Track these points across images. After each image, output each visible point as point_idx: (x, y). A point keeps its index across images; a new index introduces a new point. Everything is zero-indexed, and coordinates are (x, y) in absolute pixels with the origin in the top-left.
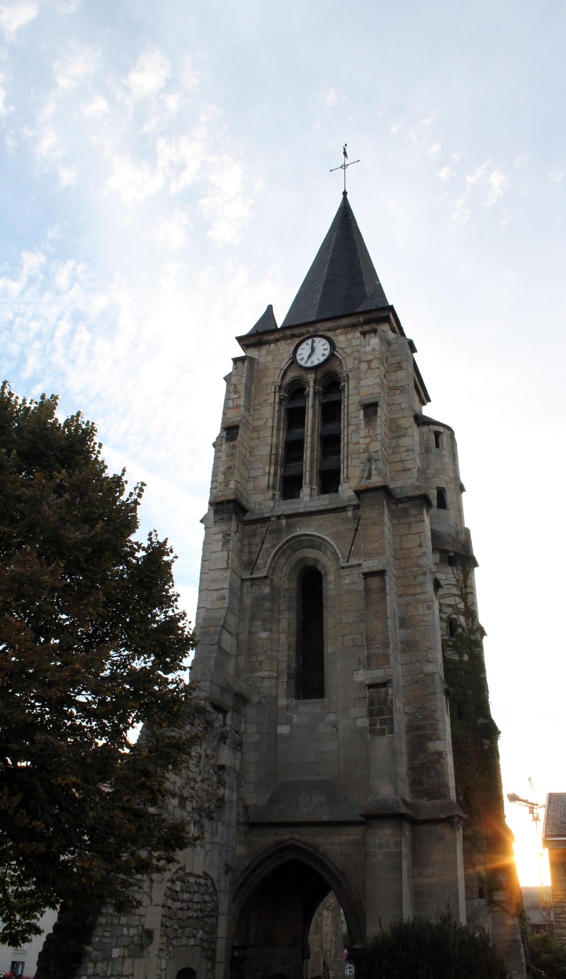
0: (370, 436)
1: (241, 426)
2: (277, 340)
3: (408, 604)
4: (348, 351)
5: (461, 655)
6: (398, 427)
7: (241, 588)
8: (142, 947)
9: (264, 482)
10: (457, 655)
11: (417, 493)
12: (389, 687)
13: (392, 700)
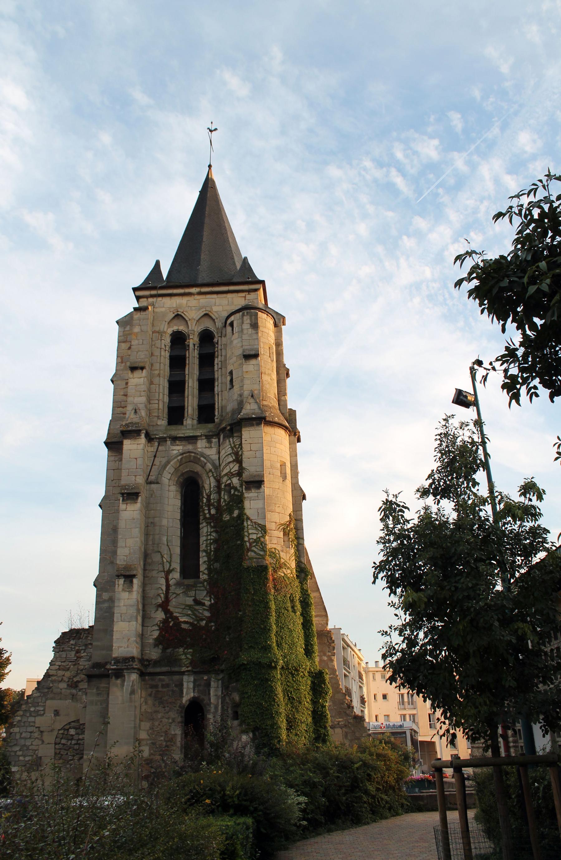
5: (231, 512)
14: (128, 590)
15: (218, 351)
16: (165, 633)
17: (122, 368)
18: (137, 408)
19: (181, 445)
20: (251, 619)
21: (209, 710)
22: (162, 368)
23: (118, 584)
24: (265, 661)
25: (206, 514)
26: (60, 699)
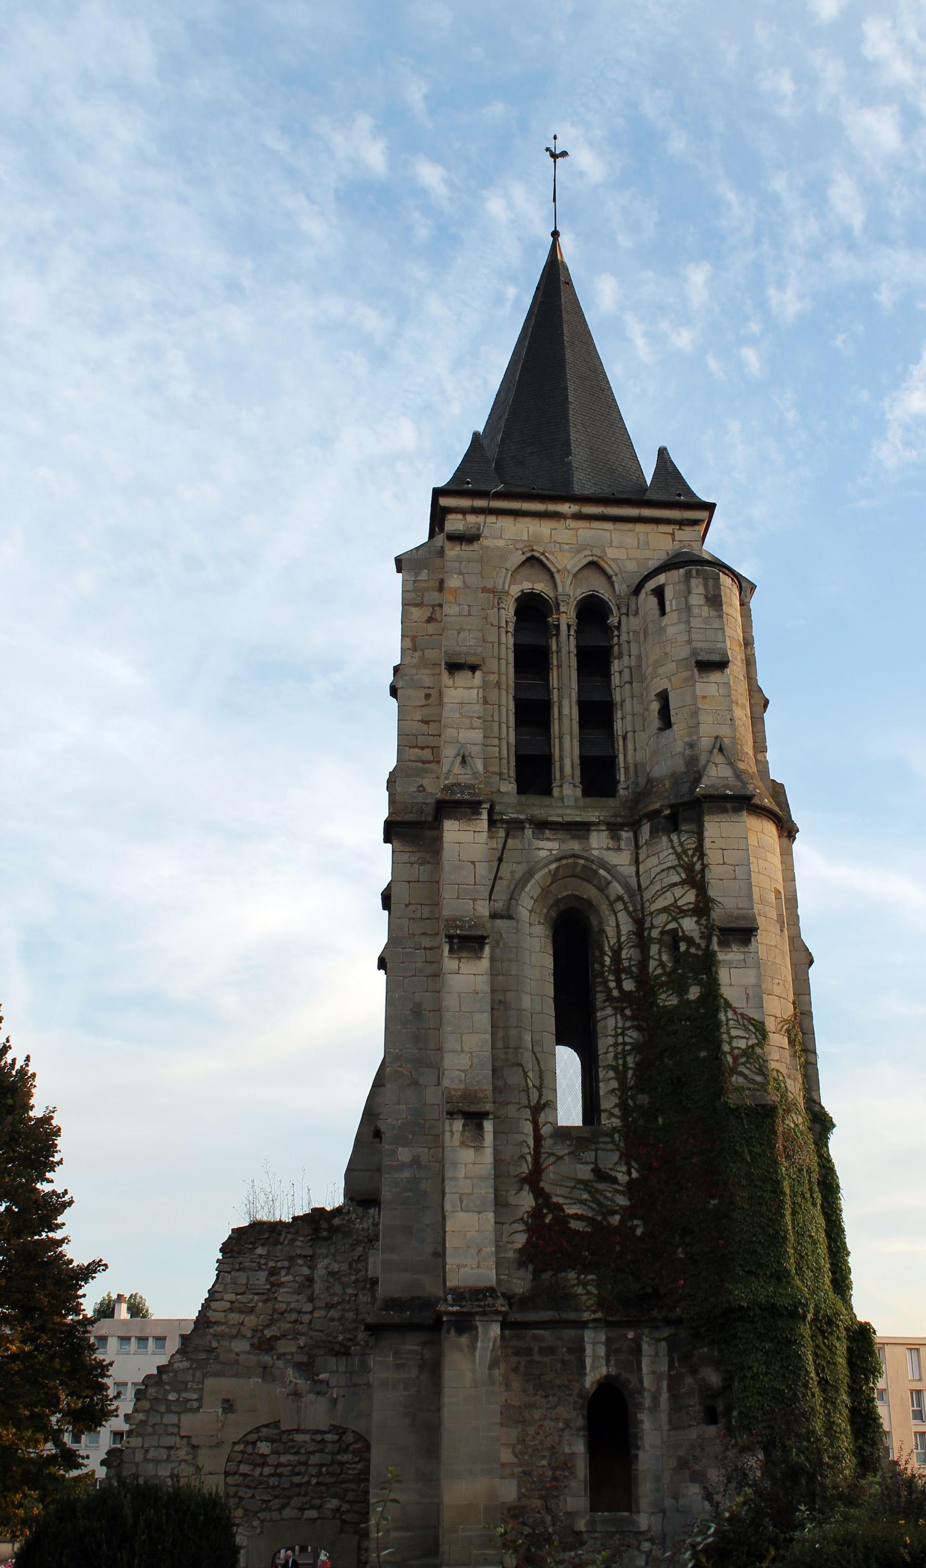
5: (682, 990)
14: (472, 1144)
15: (619, 644)
16: (537, 1239)
17: (415, 661)
18: (466, 754)
19: (555, 839)
20: (748, 1215)
21: (641, 1404)
22: (503, 670)
23: (451, 1131)
24: (782, 1302)
25: (612, 989)
26: (236, 1375)
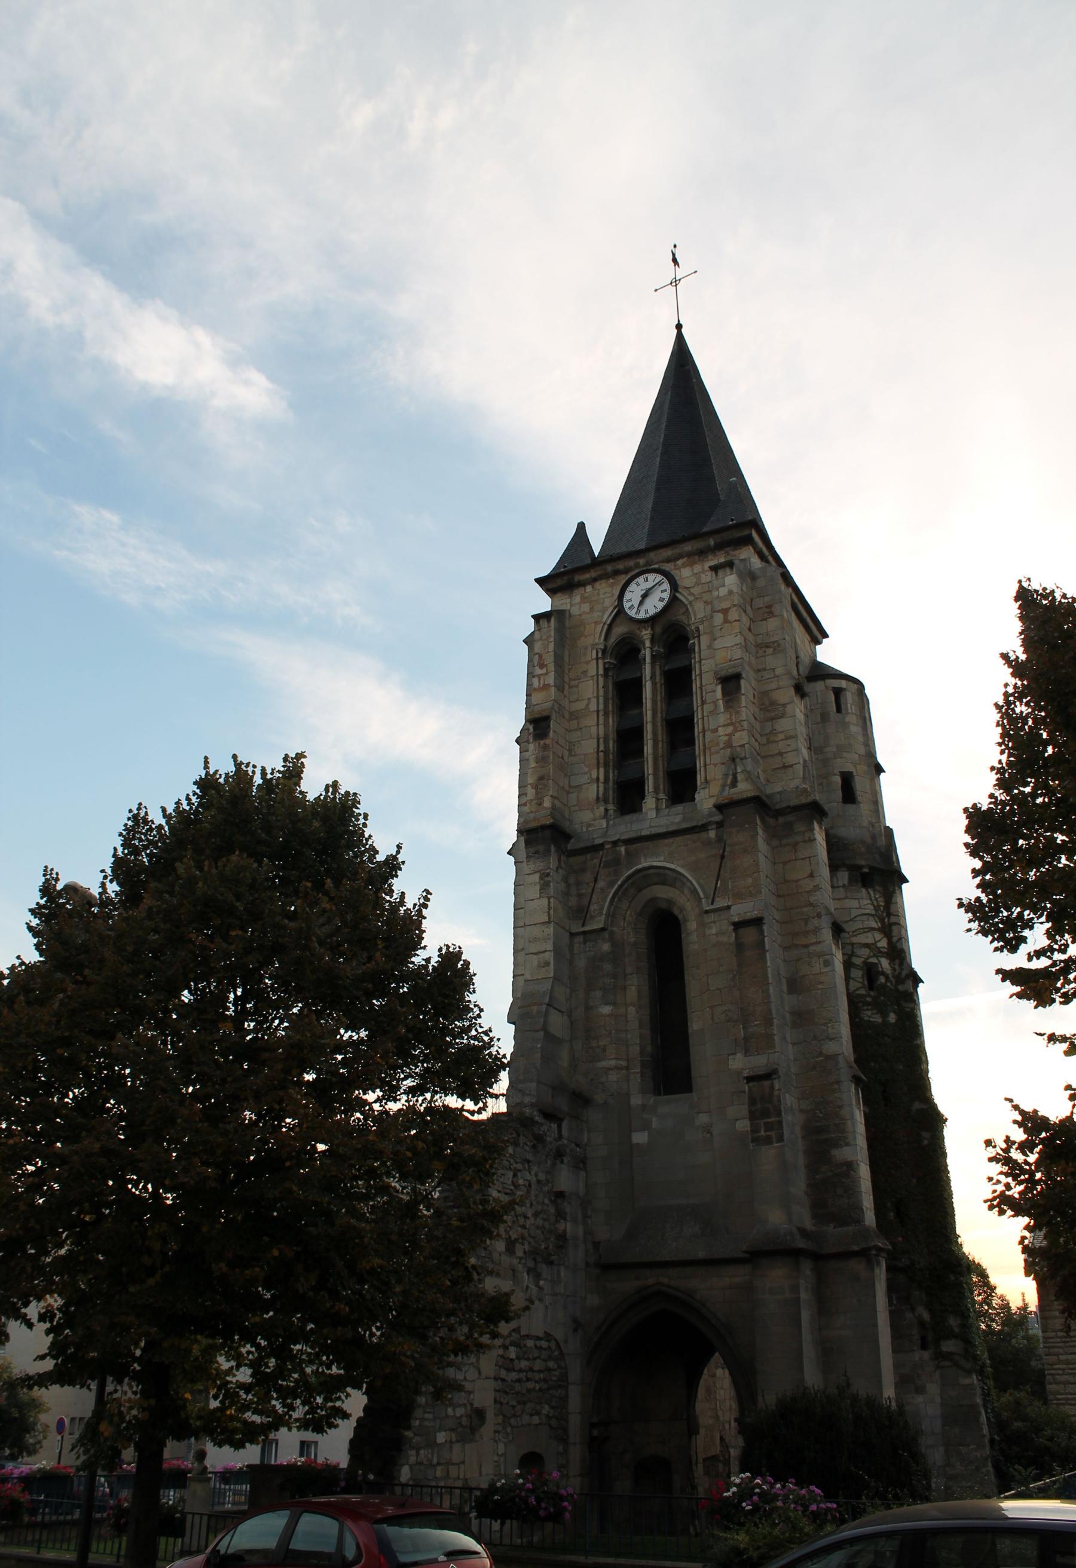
0: (731, 724)
1: (554, 716)
2: (595, 580)
3: (799, 960)
4: (696, 591)
5: (884, 1015)
6: (773, 703)
7: (571, 946)
8: (473, 1430)
9: (592, 792)
10: (879, 1015)
11: (804, 800)
12: (775, 1079)
13: (779, 1096)
